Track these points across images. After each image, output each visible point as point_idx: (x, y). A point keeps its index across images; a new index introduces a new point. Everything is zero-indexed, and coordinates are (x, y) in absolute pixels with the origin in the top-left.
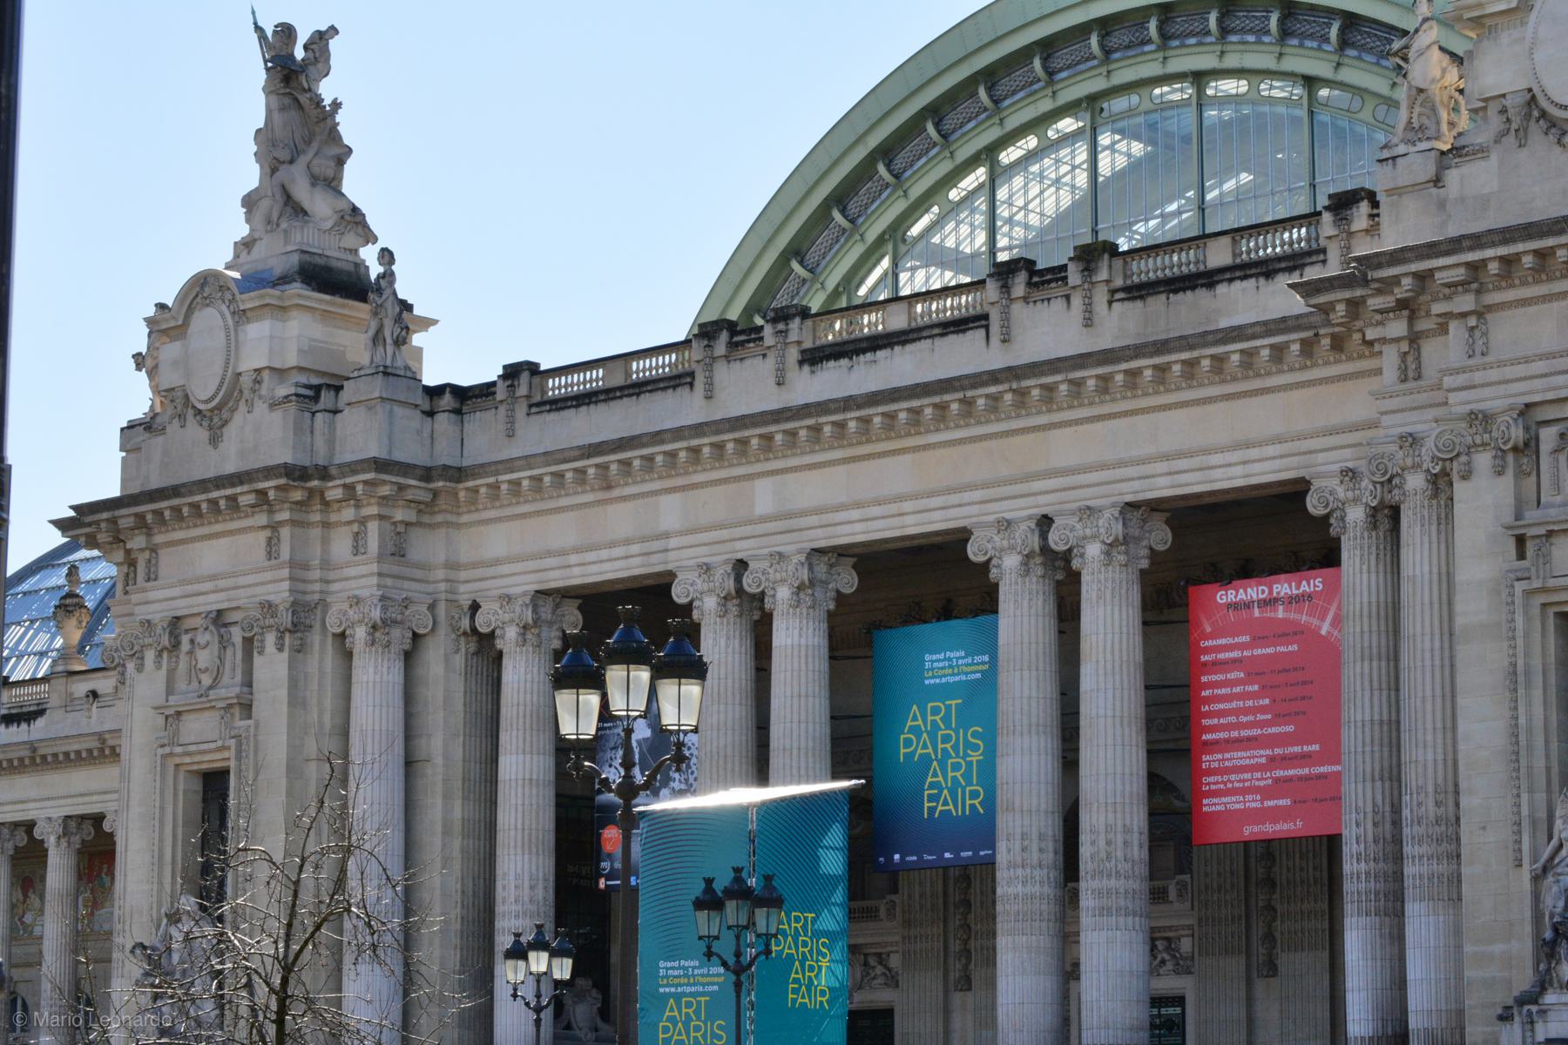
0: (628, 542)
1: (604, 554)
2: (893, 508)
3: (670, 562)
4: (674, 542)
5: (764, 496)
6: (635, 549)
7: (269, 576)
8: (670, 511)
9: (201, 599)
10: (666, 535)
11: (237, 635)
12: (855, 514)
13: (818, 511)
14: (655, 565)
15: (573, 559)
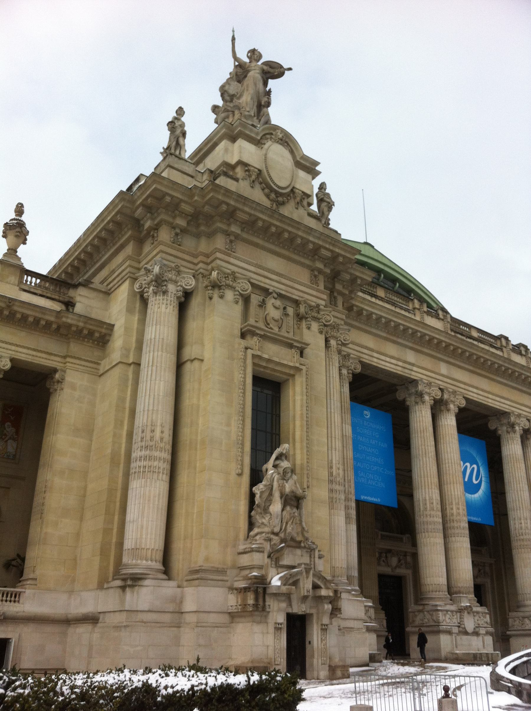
0: (398, 359)
1: (388, 359)
2: (486, 395)
3: (414, 375)
4: (415, 369)
5: (444, 369)
6: (400, 364)
7: (315, 293)
8: (411, 356)
9: (267, 281)
10: (413, 365)
11: (290, 311)
12: (475, 390)
13: (465, 384)
14: (406, 373)
15: (375, 355)
